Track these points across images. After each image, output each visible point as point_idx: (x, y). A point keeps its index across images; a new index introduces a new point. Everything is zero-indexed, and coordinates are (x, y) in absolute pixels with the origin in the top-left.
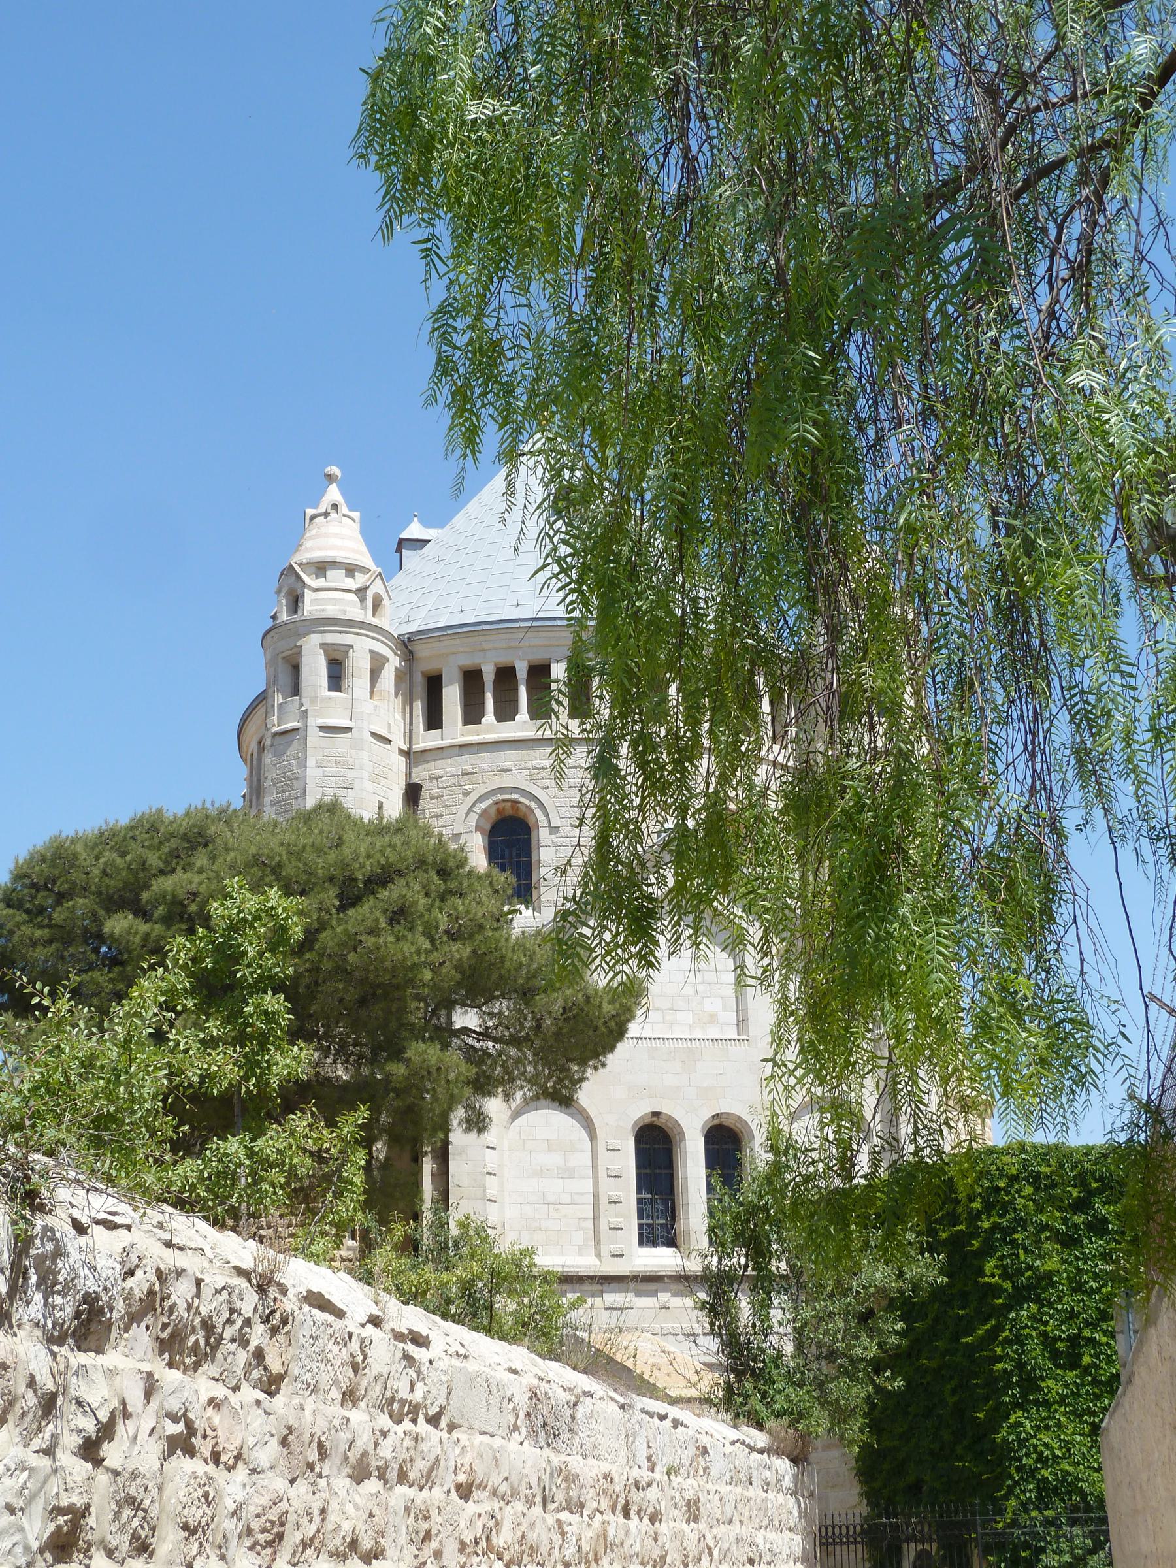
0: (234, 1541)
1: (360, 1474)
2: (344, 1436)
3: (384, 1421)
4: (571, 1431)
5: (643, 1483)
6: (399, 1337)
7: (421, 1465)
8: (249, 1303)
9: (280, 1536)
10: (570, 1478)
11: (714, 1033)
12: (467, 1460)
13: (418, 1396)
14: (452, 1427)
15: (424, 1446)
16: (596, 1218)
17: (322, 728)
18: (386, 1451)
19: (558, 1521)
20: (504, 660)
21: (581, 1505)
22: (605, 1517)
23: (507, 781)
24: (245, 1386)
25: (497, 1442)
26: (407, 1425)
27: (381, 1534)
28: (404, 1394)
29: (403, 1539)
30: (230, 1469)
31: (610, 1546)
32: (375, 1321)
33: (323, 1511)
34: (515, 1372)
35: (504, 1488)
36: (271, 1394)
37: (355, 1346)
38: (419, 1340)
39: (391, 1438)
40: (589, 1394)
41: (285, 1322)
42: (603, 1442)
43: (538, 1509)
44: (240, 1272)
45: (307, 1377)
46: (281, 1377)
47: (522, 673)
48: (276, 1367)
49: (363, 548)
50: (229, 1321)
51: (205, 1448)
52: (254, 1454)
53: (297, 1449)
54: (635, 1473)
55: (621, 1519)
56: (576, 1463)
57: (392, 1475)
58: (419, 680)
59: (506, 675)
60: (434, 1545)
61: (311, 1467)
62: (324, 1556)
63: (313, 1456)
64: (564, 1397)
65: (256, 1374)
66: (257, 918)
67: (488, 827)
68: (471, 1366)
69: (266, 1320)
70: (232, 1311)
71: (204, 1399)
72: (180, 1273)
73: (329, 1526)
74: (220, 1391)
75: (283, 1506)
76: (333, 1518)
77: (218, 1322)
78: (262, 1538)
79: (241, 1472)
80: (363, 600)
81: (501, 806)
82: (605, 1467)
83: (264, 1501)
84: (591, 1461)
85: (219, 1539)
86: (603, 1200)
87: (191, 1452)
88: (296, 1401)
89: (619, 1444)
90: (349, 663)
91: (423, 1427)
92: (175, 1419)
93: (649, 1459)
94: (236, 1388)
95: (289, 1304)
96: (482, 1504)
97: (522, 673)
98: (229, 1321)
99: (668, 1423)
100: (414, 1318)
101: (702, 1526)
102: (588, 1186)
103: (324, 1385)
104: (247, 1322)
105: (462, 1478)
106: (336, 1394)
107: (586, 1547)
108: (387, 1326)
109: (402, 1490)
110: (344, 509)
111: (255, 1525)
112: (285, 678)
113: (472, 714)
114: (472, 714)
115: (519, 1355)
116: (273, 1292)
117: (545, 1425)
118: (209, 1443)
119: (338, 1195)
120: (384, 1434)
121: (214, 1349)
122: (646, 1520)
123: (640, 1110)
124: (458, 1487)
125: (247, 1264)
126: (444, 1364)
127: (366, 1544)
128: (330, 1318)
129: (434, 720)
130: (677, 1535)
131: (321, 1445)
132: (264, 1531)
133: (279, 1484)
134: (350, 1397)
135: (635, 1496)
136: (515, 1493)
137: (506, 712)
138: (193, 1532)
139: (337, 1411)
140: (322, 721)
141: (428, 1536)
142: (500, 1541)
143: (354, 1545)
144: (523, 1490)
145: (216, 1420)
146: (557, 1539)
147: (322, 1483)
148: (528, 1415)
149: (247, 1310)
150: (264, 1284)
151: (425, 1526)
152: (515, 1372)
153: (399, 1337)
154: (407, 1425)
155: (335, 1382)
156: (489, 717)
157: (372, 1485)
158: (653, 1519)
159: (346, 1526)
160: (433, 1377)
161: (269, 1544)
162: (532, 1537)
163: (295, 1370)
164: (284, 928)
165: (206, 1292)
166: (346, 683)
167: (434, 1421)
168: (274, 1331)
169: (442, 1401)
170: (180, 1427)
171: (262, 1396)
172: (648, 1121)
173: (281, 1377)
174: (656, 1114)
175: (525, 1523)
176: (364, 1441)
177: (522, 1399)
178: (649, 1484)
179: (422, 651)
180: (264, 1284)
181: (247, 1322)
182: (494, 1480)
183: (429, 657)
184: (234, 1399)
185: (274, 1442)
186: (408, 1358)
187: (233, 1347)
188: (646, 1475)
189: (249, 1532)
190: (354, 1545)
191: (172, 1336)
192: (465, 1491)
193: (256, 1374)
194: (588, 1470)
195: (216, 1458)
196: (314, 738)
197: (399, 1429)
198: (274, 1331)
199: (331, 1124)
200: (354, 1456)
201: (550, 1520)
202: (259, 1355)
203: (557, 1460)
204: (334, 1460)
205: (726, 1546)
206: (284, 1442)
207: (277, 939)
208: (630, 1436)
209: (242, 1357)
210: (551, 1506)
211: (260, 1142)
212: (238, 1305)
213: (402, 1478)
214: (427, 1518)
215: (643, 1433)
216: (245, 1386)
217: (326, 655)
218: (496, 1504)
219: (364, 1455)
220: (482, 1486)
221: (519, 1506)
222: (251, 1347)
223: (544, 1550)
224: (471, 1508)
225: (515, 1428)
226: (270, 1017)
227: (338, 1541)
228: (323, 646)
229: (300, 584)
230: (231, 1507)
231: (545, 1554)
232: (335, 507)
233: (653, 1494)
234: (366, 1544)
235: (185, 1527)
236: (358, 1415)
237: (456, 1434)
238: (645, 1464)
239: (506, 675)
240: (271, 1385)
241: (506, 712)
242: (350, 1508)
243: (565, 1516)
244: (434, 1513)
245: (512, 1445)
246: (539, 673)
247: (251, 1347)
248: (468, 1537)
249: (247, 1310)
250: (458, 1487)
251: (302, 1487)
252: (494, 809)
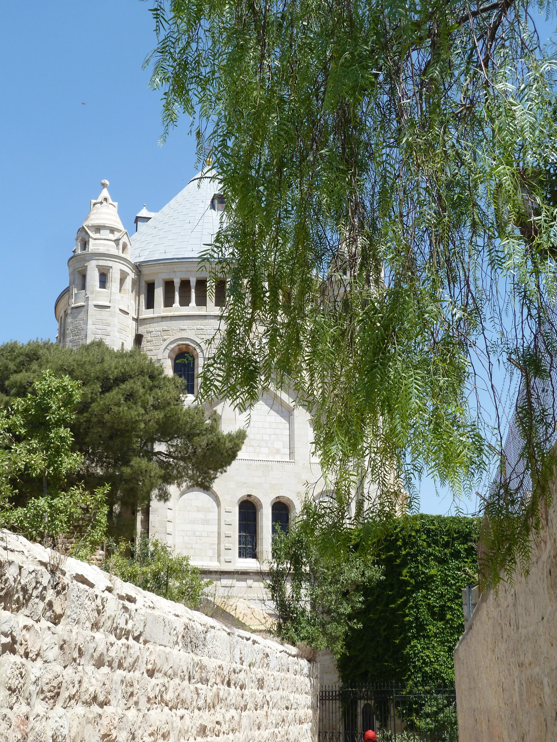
0: (34, 696)
1: (99, 664)
2: (92, 645)
3: (112, 638)
4: (204, 645)
5: (237, 671)
6: (121, 597)
7: (130, 660)
8: (46, 579)
9: (58, 694)
10: (202, 668)
11: (278, 458)
12: (152, 658)
13: (129, 626)
14: (145, 642)
15: (131, 651)
16: (219, 544)
17: (96, 306)
18: (112, 653)
19: (196, 688)
20: (185, 277)
21: (207, 681)
22: (219, 686)
23: (184, 335)
24: (42, 619)
25: (168, 650)
26: (123, 640)
27: (109, 693)
28: (122, 625)
29: (120, 696)
30: (34, 660)
31: (220, 700)
32: (109, 590)
33: (80, 682)
34: (178, 616)
35: (170, 672)
36: (56, 624)
37: (99, 601)
38: (131, 599)
39: (115, 647)
40: (213, 627)
41: (64, 589)
42: (219, 650)
43: (186, 682)
44: (42, 563)
45: (74, 616)
46: (61, 616)
47: (193, 283)
48: (58, 611)
49: (119, 220)
50: (36, 588)
51: (21, 650)
52: (46, 653)
53: (67, 651)
54: (234, 665)
55: (226, 687)
56: (205, 660)
57: (115, 665)
58: (143, 285)
59: (185, 284)
60: (135, 699)
61: (75, 660)
62: (80, 704)
63: (76, 655)
64: (201, 628)
65: (48, 614)
66: (58, 390)
67: (174, 356)
68: (156, 612)
69: (54, 587)
70: (37, 583)
71: (21, 625)
72: (11, 563)
73: (83, 689)
74: (29, 622)
75: (60, 679)
76: (85, 685)
77: (30, 588)
78: (49, 695)
79: (39, 662)
80: (118, 245)
81: (181, 347)
82: (219, 662)
83: (50, 676)
84: (213, 659)
85: (27, 695)
86: (223, 536)
87: (14, 652)
88: (68, 627)
89: (227, 652)
90: (110, 275)
91: (131, 642)
92: (6, 635)
93: (241, 659)
94: (38, 621)
95: (66, 580)
96: (159, 679)
97: (193, 283)
98: (36, 588)
99: (250, 642)
100: (129, 589)
101: (265, 691)
102: (215, 528)
103: (82, 620)
104: (45, 588)
105: (150, 667)
106: (88, 624)
107: (209, 701)
108: (115, 592)
109: (120, 672)
110: (110, 201)
111: (46, 688)
112: (78, 281)
113: (169, 302)
114: (169, 302)
115: (180, 608)
116: (58, 574)
117: (191, 642)
118: (23, 647)
119: (93, 527)
120: (112, 645)
121: (28, 601)
122: (238, 688)
123: (241, 494)
124: (148, 671)
125: (46, 560)
126: (142, 611)
127: (101, 698)
128: (87, 587)
129: (150, 304)
130: (253, 695)
131: (80, 649)
132: (50, 691)
133: (57, 668)
134: (95, 626)
135: (233, 677)
136: (175, 674)
137: (185, 302)
138: (14, 691)
139: (89, 633)
140: (96, 303)
141: (132, 694)
142: (167, 697)
143: (95, 698)
144: (179, 673)
145: (27, 636)
146: (195, 696)
147: (80, 668)
148: (183, 637)
149: (45, 582)
150: (54, 570)
151: (131, 690)
152: (178, 616)
153: (121, 597)
154: (123, 640)
155: (88, 619)
157: (105, 669)
158: (242, 687)
159: (91, 689)
160: (137, 617)
161: (52, 697)
162: (183, 696)
163: (68, 612)
164: (71, 396)
165: (24, 573)
166: (108, 285)
167: (137, 639)
168: (58, 593)
169: (141, 629)
170: (9, 640)
171: (51, 625)
172: (245, 498)
173: (61, 616)
174: (249, 496)
175: (180, 689)
176: (102, 648)
177: (180, 630)
178: (240, 671)
179: (145, 271)
180: (54, 570)
181: (45, 588)
182: (166, 668)
183: (148, 274)
184: (37, 626)
185: (57, 648)
186: (125, 608)
187: (37, 600)
188: (238, 667)
189: (42, 691)
190: (95, 698)
191: (6, 594)
192: (151, 673)
193: (48, 614)
194: (211, 663)
195: (26, 655)
196: (92, 310)
197: (120, 642)
198: (58, 593)
199: (92, 493)
200: (96, 655)
201: (192, 687)
202: (50, 605)
203: (197, 659)
204: (86, 657)
205: (276, 701)
206: (61, 648)
207: (67, 401)
208: (232, 648)
209: (42, 605)
210: (193, 681)
211: (56, 500)
212: (40, 580)
213: (120, 666)
214: (132, 686)
215: (238, 646)
216: (42, 619)
217: (99, 271)
218: (166, 679)
219: (102, 654)
220: (159, 671)
221: (177, 680)
222: (46, 601)
223: (188, 702)
224: (154, 681)
225: (177, 643)
226: (62, 439)
227: (87, 697)
228: (97, 266)
229: (87, 236)
230: (34, 679)
231: (189, 704)
232: (106, 199)
233: (242, 675)
234: (101, 698)
235: (10, 689)
236: (99, 635)
237: (148, 645)
238: (239, 661)
239: (185, 284)
240: (56, 620)
241: (185, 302)
242: (93, 681)
243: (199, 685)
244: (135, 684)
245: (175, 651)
246: (201, 284)
247: (46, 601)
248: (152, 695)
249: (45, 582)
250: (148, 671)
251: (70, 670)
252: (178, 347)
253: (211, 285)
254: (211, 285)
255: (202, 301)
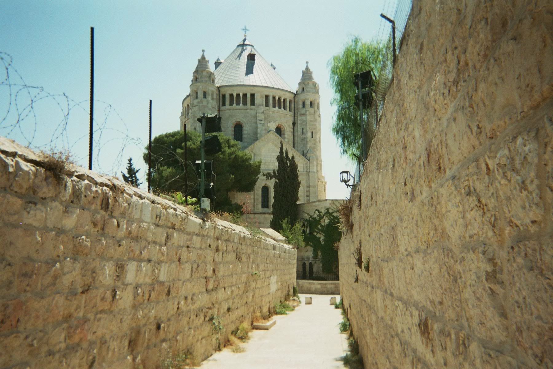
16: (254, 203)
20: (238, 92)
58: (221, 96)
86: (255, 200)
113: (231, 104)
114: (231, 104)
129: (224, 105)
137: (238, 104)
156: (235, 105)
166: (207, 97)
174: (266, 184)
183: (223, 91)
239: (238, 95)
241: (238, 104)
253: (249, 96)
254: (249, 96)
255: (245, 103)
